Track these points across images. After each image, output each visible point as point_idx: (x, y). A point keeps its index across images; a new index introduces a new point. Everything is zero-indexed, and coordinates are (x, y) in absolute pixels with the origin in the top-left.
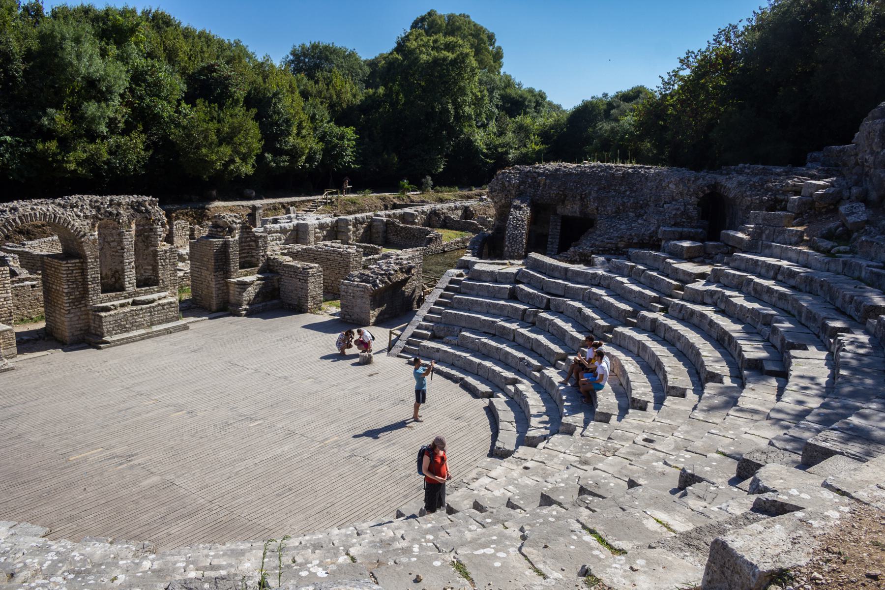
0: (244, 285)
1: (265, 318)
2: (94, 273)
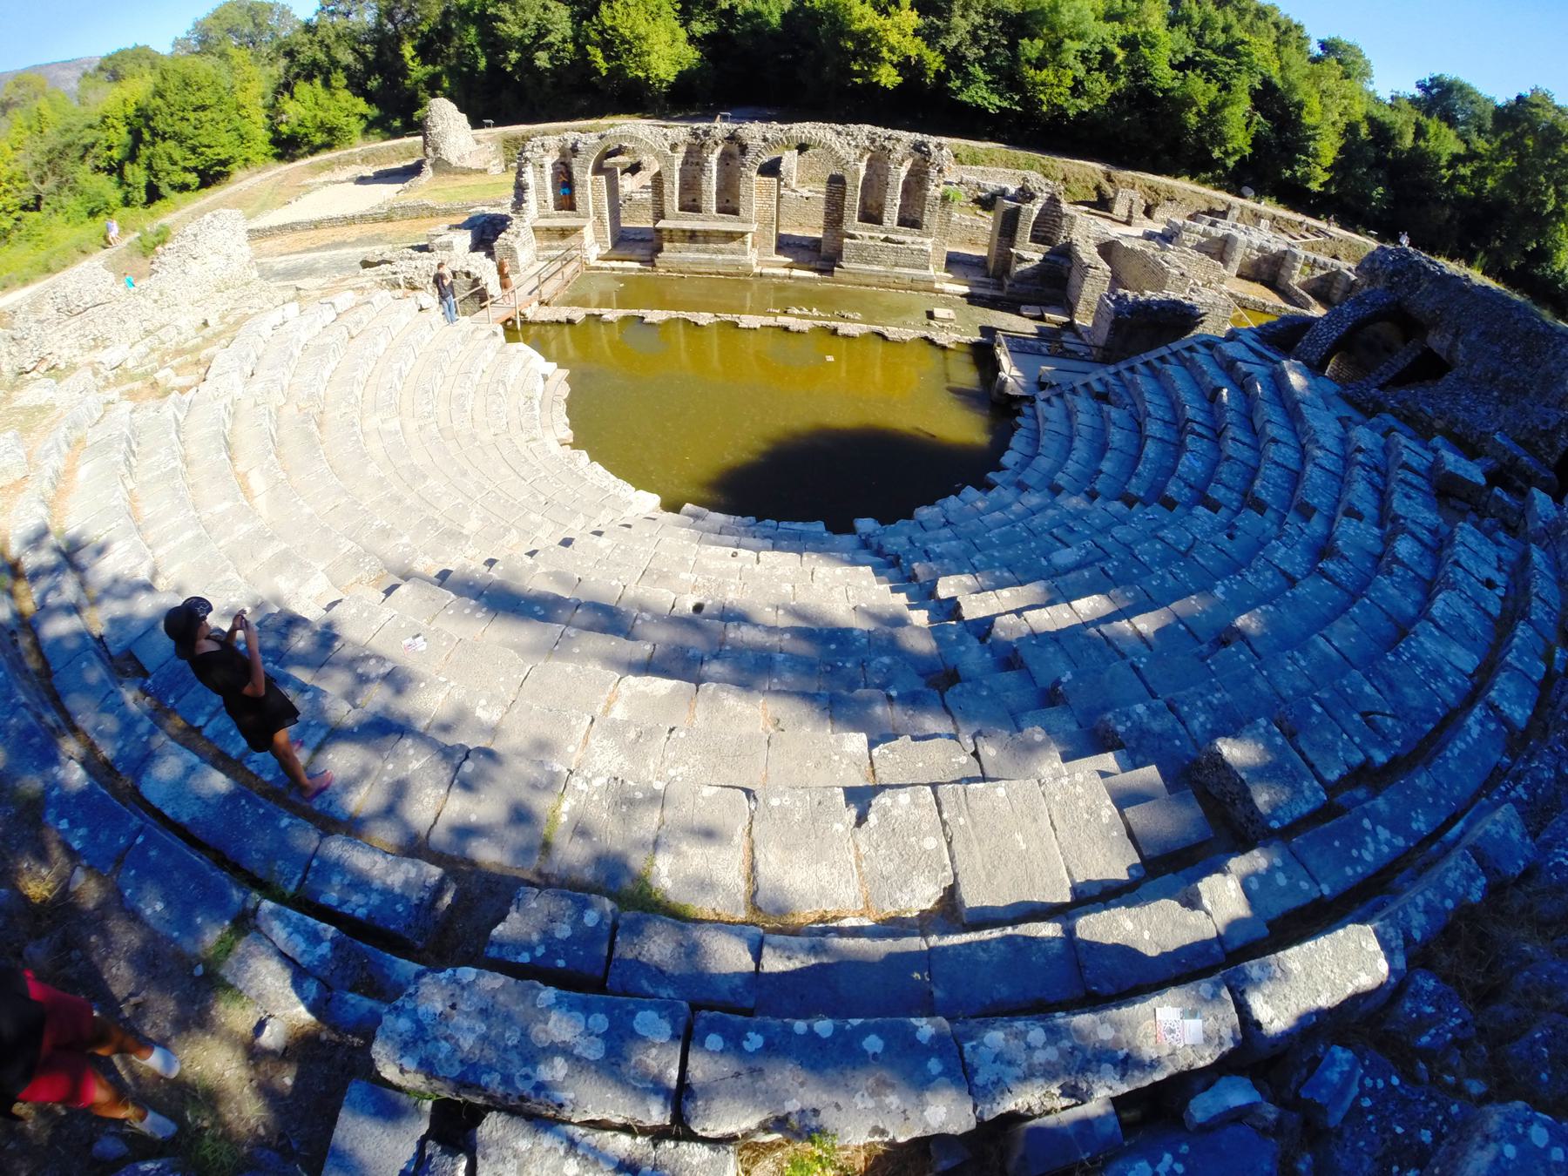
0: (1021, 259)
2: (854, 199)
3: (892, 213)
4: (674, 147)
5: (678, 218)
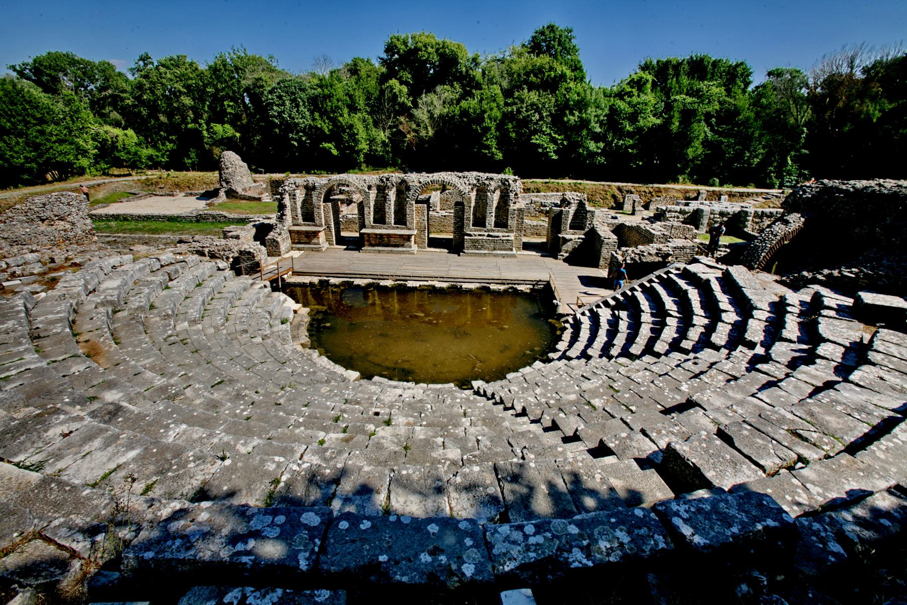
0: (565, 241)
1: (570, 265)
2: (469, 214)
3: (491, 220)
4: (370, 187)
5: (373, 227)
